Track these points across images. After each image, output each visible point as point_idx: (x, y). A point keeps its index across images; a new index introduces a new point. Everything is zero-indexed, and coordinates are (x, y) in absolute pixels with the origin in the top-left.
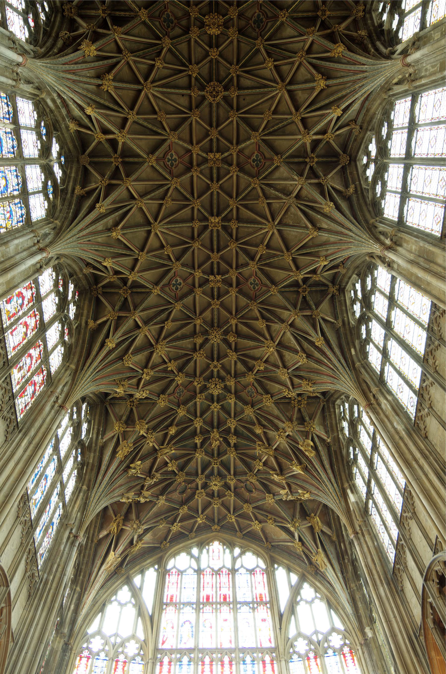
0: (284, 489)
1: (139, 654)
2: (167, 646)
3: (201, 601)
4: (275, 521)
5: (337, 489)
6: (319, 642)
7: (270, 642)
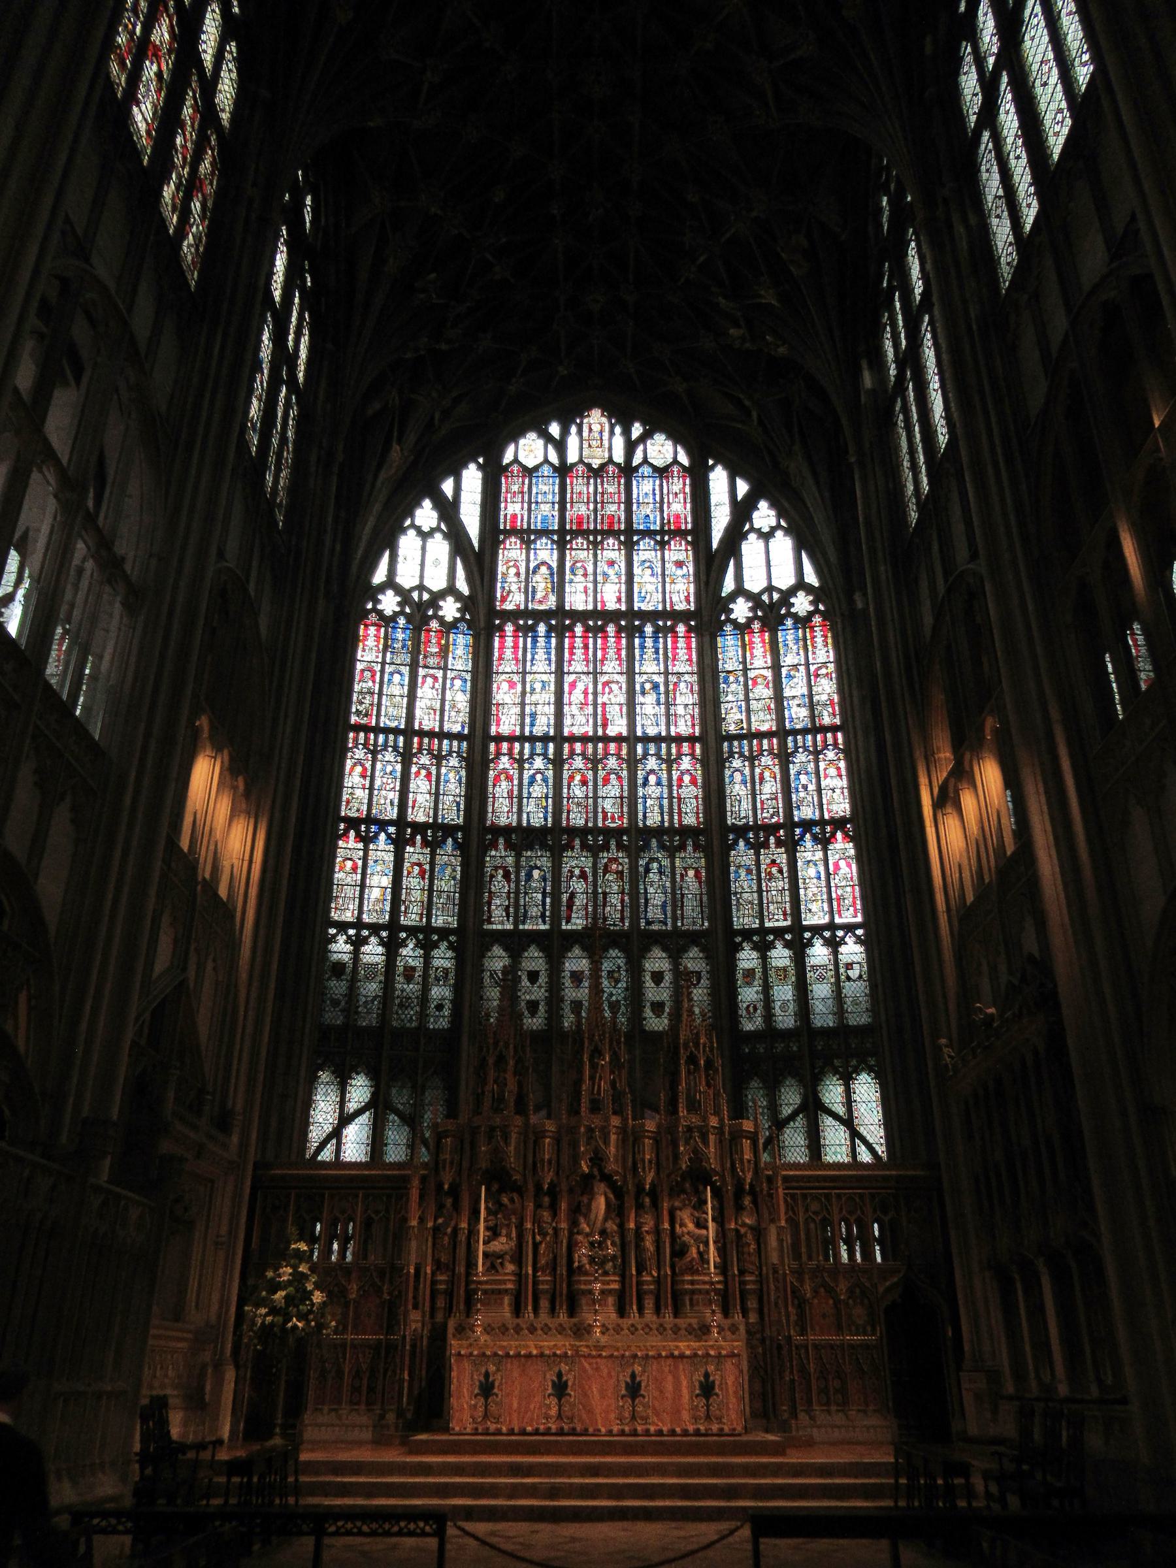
0: (737, 325)
1: (462, 619)
2: (509, 606)
3: (568, 527)
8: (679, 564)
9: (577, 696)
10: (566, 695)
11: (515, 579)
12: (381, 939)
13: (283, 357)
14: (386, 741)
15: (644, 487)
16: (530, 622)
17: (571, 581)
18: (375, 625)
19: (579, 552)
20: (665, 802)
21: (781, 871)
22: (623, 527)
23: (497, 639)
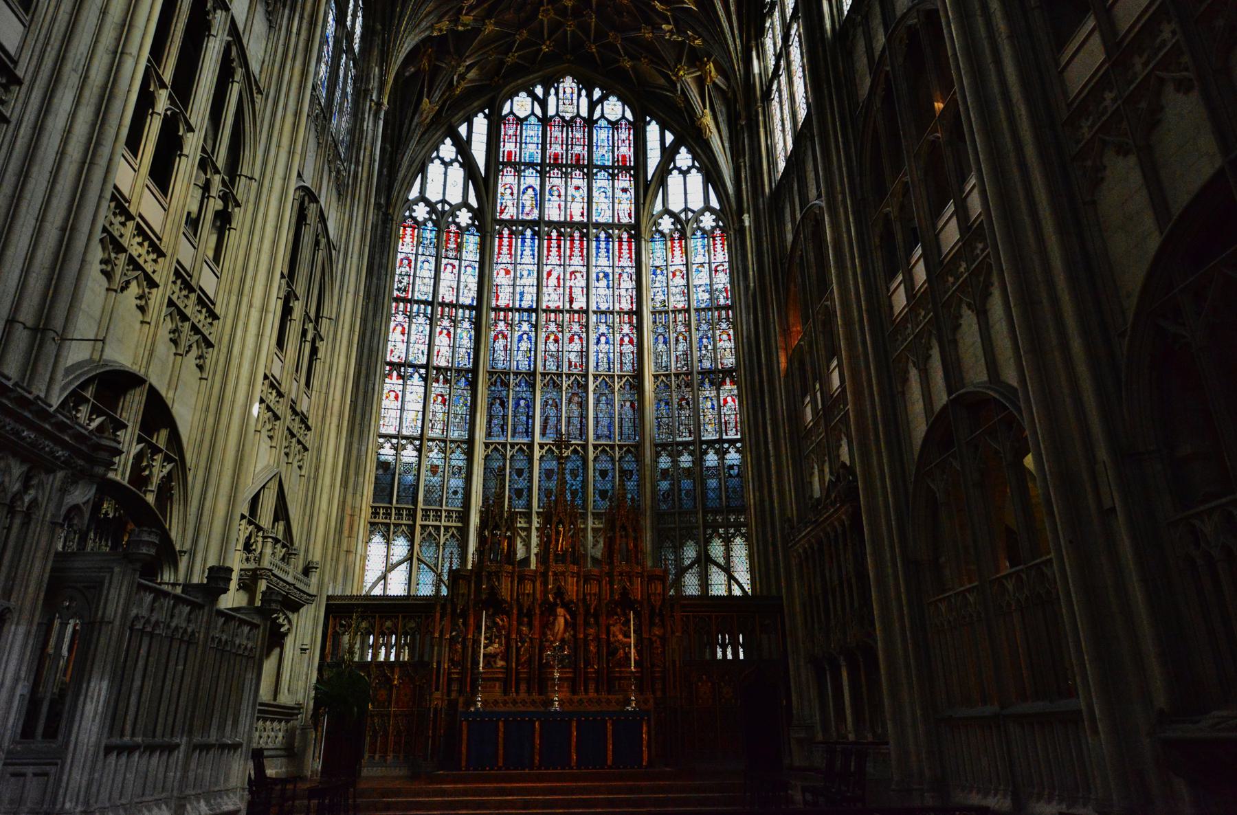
1: (473, 224)
2: (506, 216)
4: (652, 61)
5: (739, 48)
6: (688, 221)
7: (630, 218)
8: (625, 190)
9: (553, 281)
10: (545, 280)
11: (510, 197)
12: (415, 446)
13: (344, 34)
14: (419, 309)
15: (602, 135)
16: (520, 228)
17: (549, 200)
18: (411, 227)
19: (555, 181)
20: (611, 355)
21: (688, 403)
22: (586, 163)
23: (497, 240)
